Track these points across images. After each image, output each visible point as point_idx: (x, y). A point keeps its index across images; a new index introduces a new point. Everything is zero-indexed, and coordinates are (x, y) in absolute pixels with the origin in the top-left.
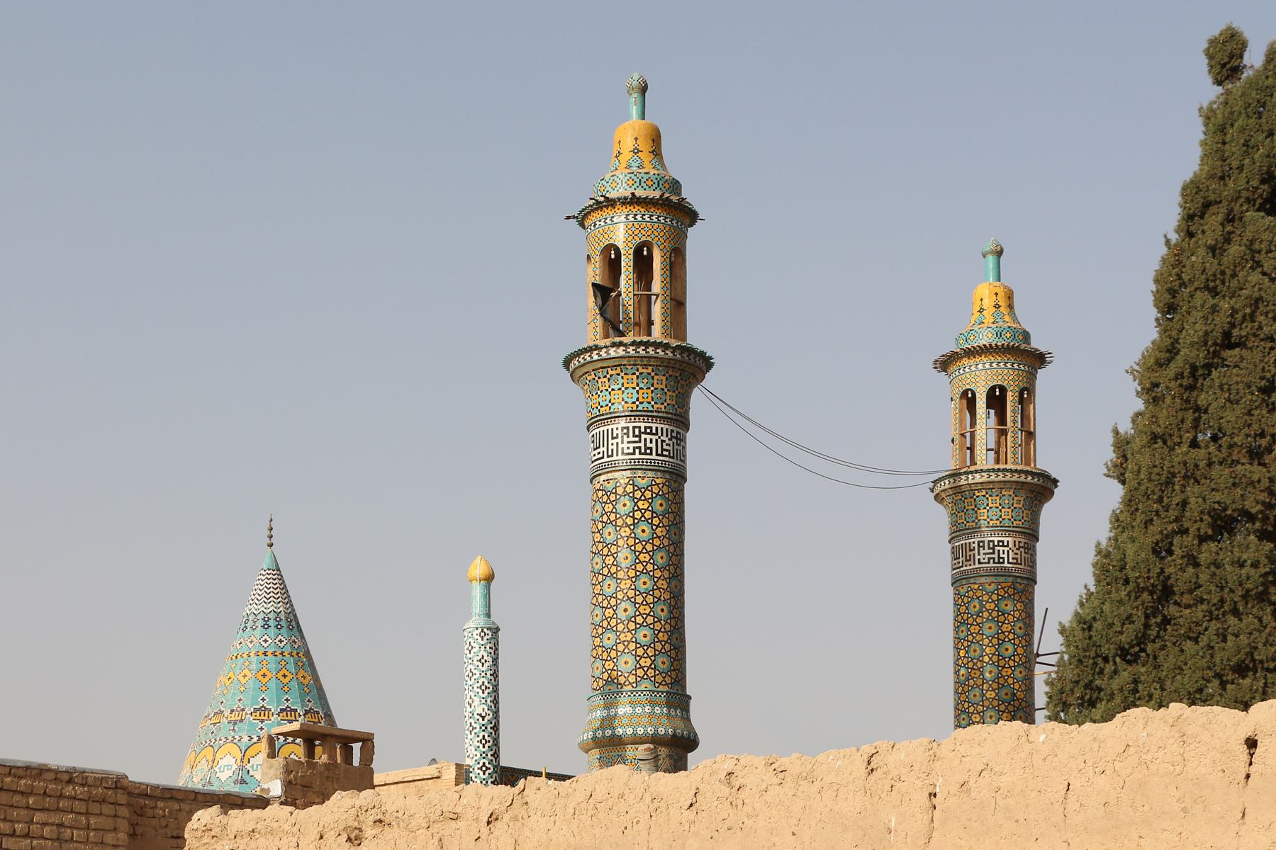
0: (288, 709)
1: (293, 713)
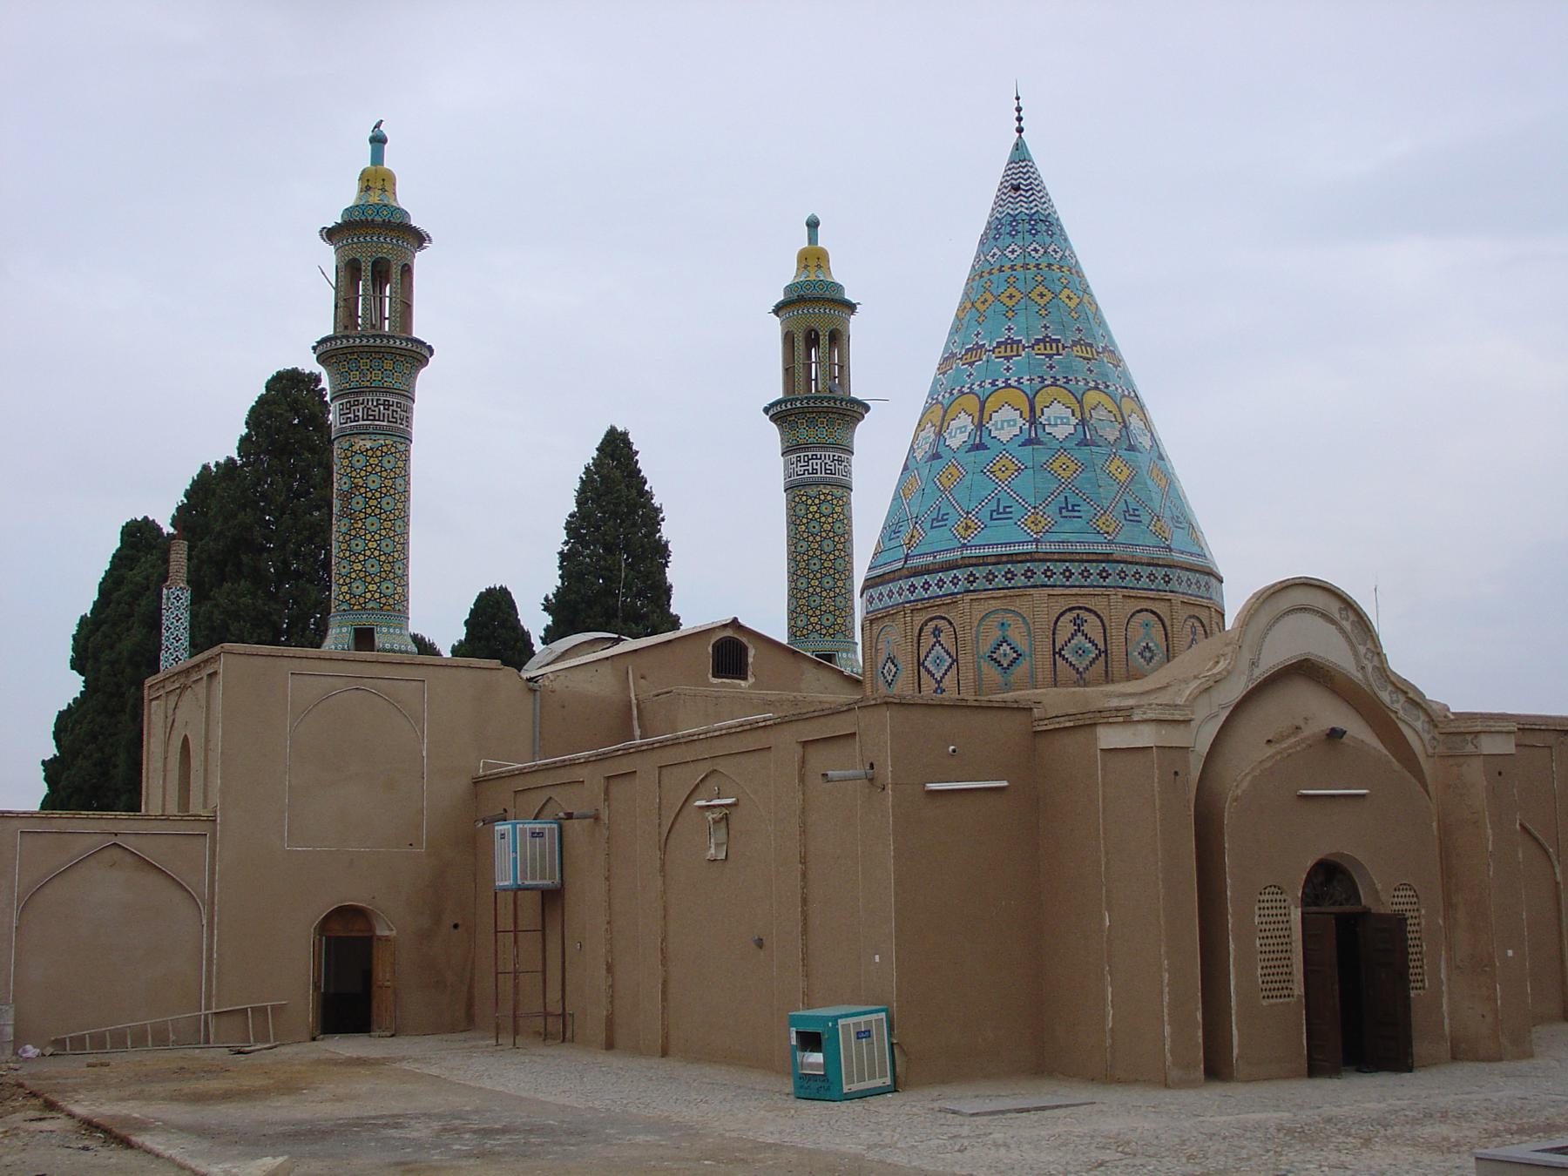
0: (1048, 340)
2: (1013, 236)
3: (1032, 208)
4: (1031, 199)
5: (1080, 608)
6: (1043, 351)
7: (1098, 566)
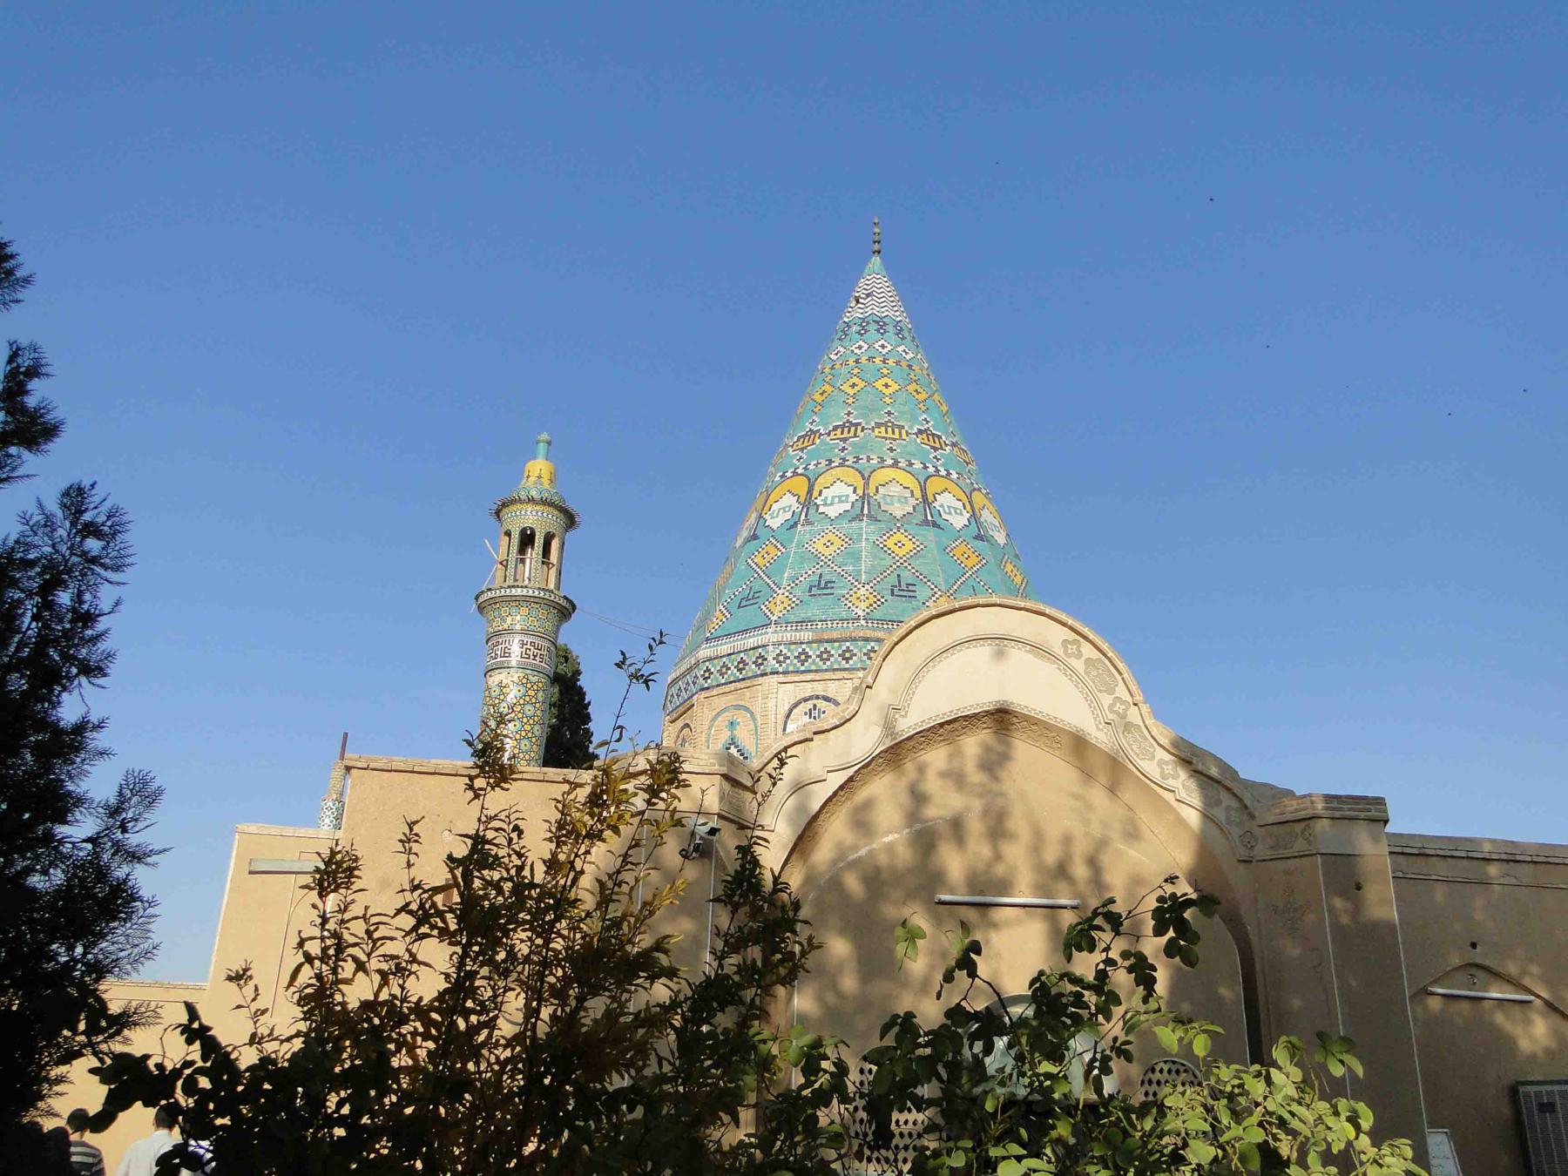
0: (890, 424)
1: (896, 430)
2: (862, 335)
3: (883, 312)
4: (882, 305)
5: (817, 697)
6: (883, 434)
7: (840, 646)
